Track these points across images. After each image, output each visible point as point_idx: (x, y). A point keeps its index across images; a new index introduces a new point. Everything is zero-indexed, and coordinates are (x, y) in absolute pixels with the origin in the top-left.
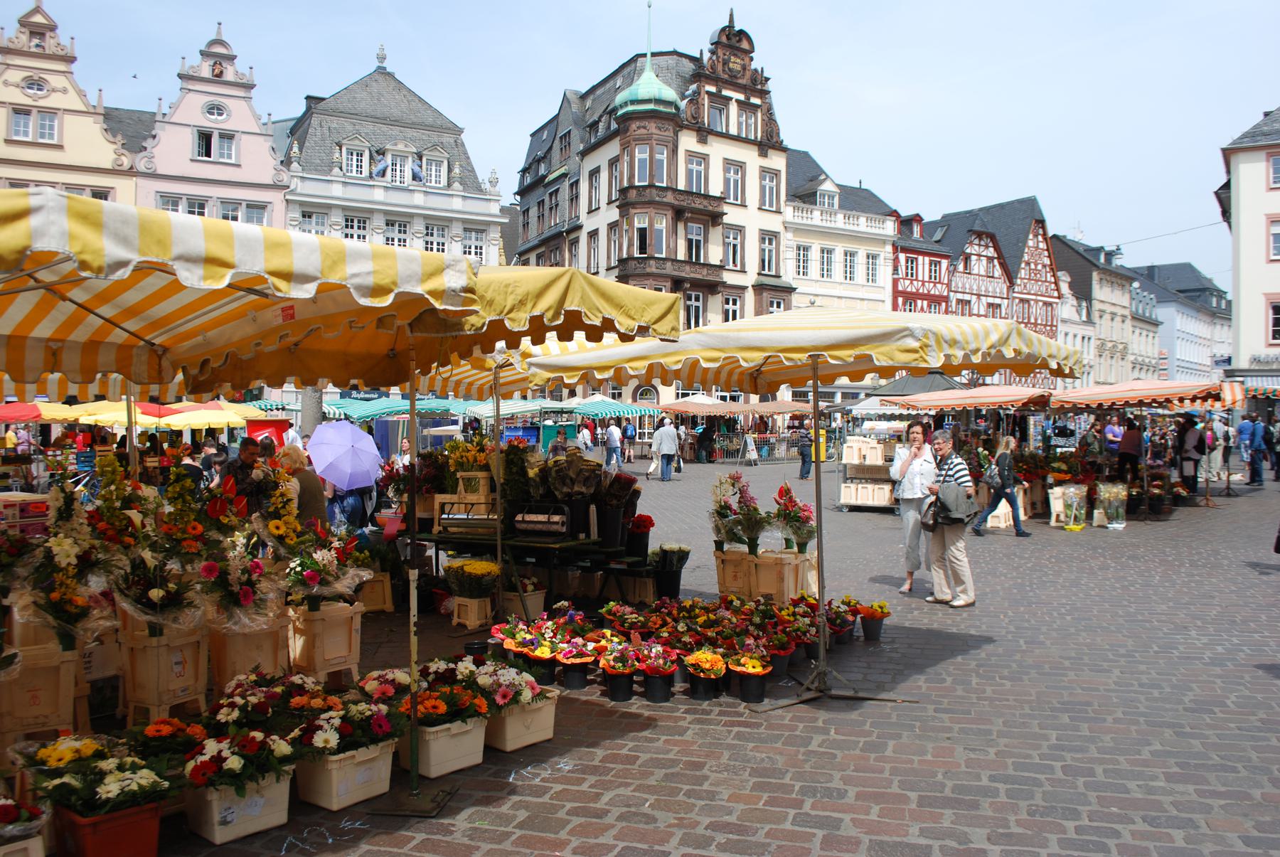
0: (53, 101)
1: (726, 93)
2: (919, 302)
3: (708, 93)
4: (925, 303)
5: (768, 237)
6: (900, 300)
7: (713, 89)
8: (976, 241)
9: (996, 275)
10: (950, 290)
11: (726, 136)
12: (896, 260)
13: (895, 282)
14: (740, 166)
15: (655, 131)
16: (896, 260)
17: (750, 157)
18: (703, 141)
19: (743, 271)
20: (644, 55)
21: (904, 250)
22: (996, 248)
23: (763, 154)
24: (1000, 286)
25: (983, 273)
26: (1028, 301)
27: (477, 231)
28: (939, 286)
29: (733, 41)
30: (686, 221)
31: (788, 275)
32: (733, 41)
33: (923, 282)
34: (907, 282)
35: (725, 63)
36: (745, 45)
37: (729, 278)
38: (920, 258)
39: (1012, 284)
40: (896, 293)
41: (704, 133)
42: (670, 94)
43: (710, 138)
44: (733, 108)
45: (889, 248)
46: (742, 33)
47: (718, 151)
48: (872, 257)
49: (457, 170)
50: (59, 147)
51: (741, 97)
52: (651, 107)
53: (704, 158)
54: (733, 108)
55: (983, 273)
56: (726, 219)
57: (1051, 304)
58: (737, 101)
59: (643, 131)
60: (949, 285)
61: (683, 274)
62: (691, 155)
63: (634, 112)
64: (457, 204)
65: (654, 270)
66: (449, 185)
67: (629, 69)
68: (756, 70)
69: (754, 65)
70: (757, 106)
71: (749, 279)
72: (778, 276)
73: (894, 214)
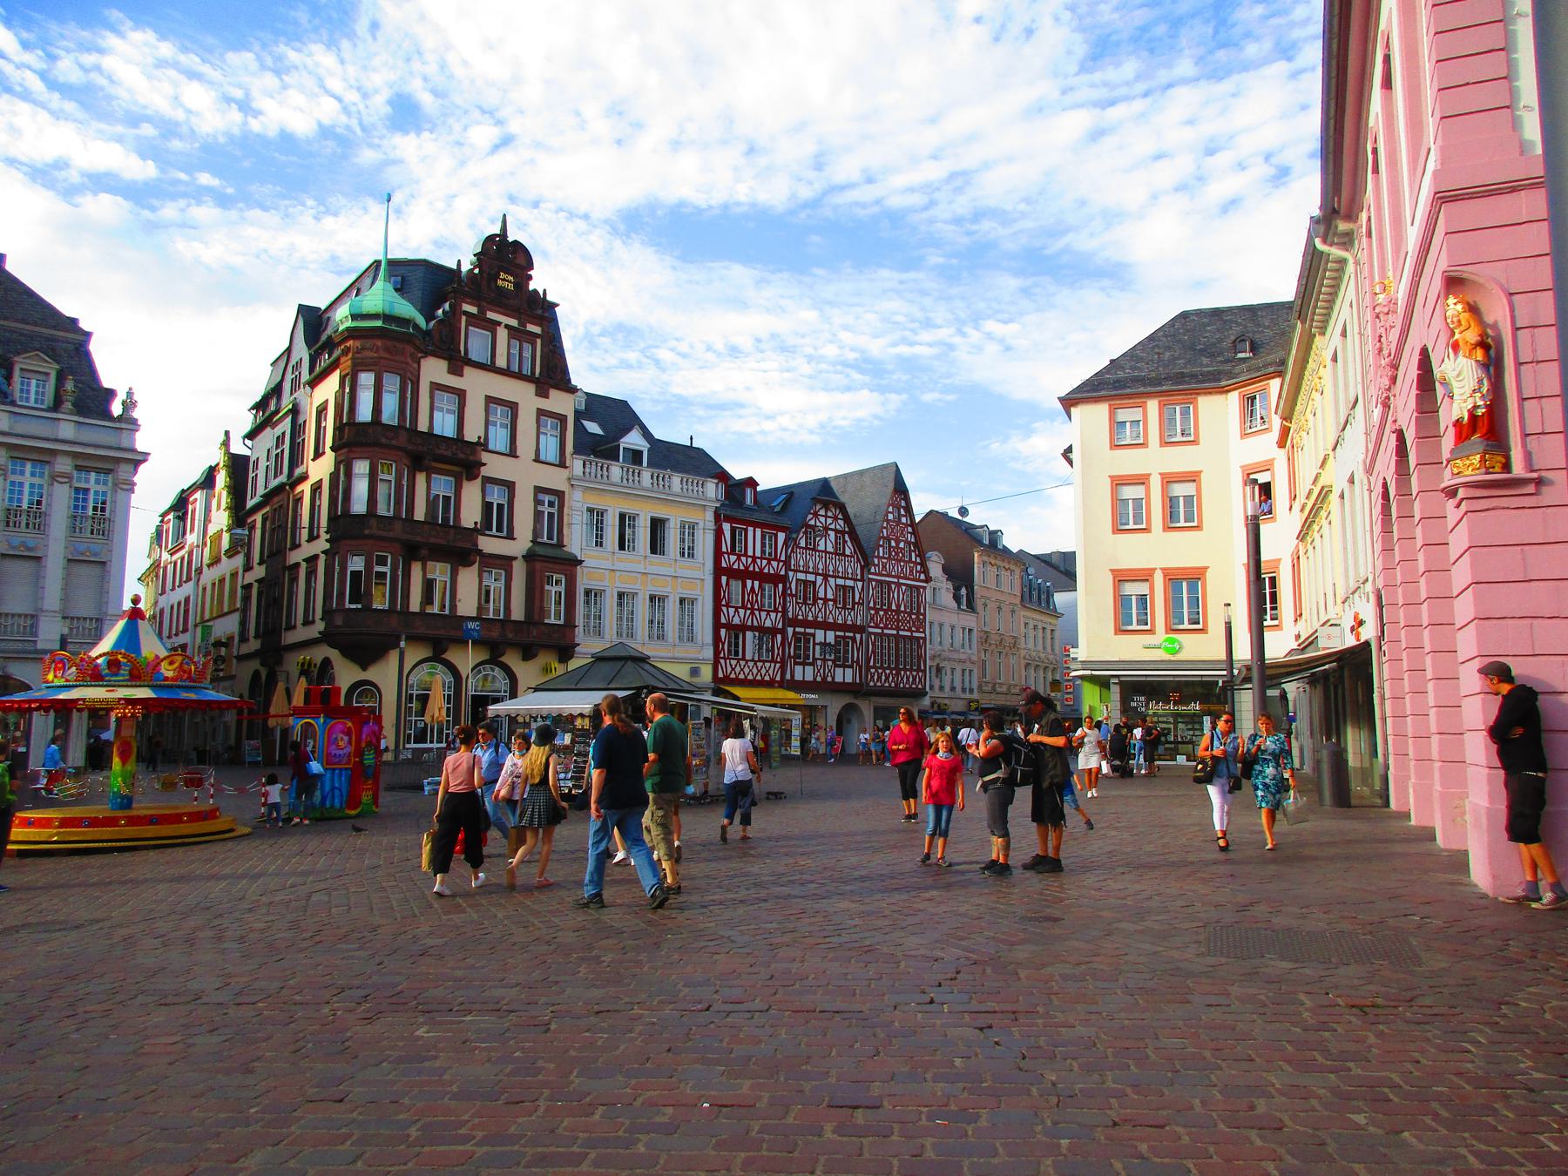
1: (491, 315)
2: (749, 583)
3: (466, 313)
4: (756, 583)
6: (724, 579)
7: (473, 310)
8: (822, 512)
9: (848, 552)
10: (788, 568)
11: (491, 368)
13: (718, 554)
14: (513, 407)
16: (719, 533)
17: (523, 394)
18: (456, 370)
19: (510, 536)
21: (728, 519)
22: (847, 519)
23: (542, 393)
24: (853, 567)
25: (830, 549)
26: (889, 583)
27: (98, 471)
28: (774, 564)
30: (430, 472)
33: (754, 558)
34: (733, 558)
37: (488, 545)
38: (751, 529)
39: (866, 566)
40: (718, 571)
41: (458, 363)
42: (405, 309)
43: (468, 370)
44: (502, 334)
45: (710, 516)
47: (477, 384)
49: (69, 386)
51: (514, 323)
52: (379, 323)
53: (461, 394)
54: (502, 334)
55: (830, 549)
56: (484, 471)
57: (918, 588)
58: (507, 326)
60: (787, 563)
61: (418, 539)
62: (436, 387)
64: (67, 430)
65: (374, 531)
66: (57, 406)
68: (535, 291)
69: (532, 286)
70: (536, 335)
72: (560, 545)
73: (723, 476)
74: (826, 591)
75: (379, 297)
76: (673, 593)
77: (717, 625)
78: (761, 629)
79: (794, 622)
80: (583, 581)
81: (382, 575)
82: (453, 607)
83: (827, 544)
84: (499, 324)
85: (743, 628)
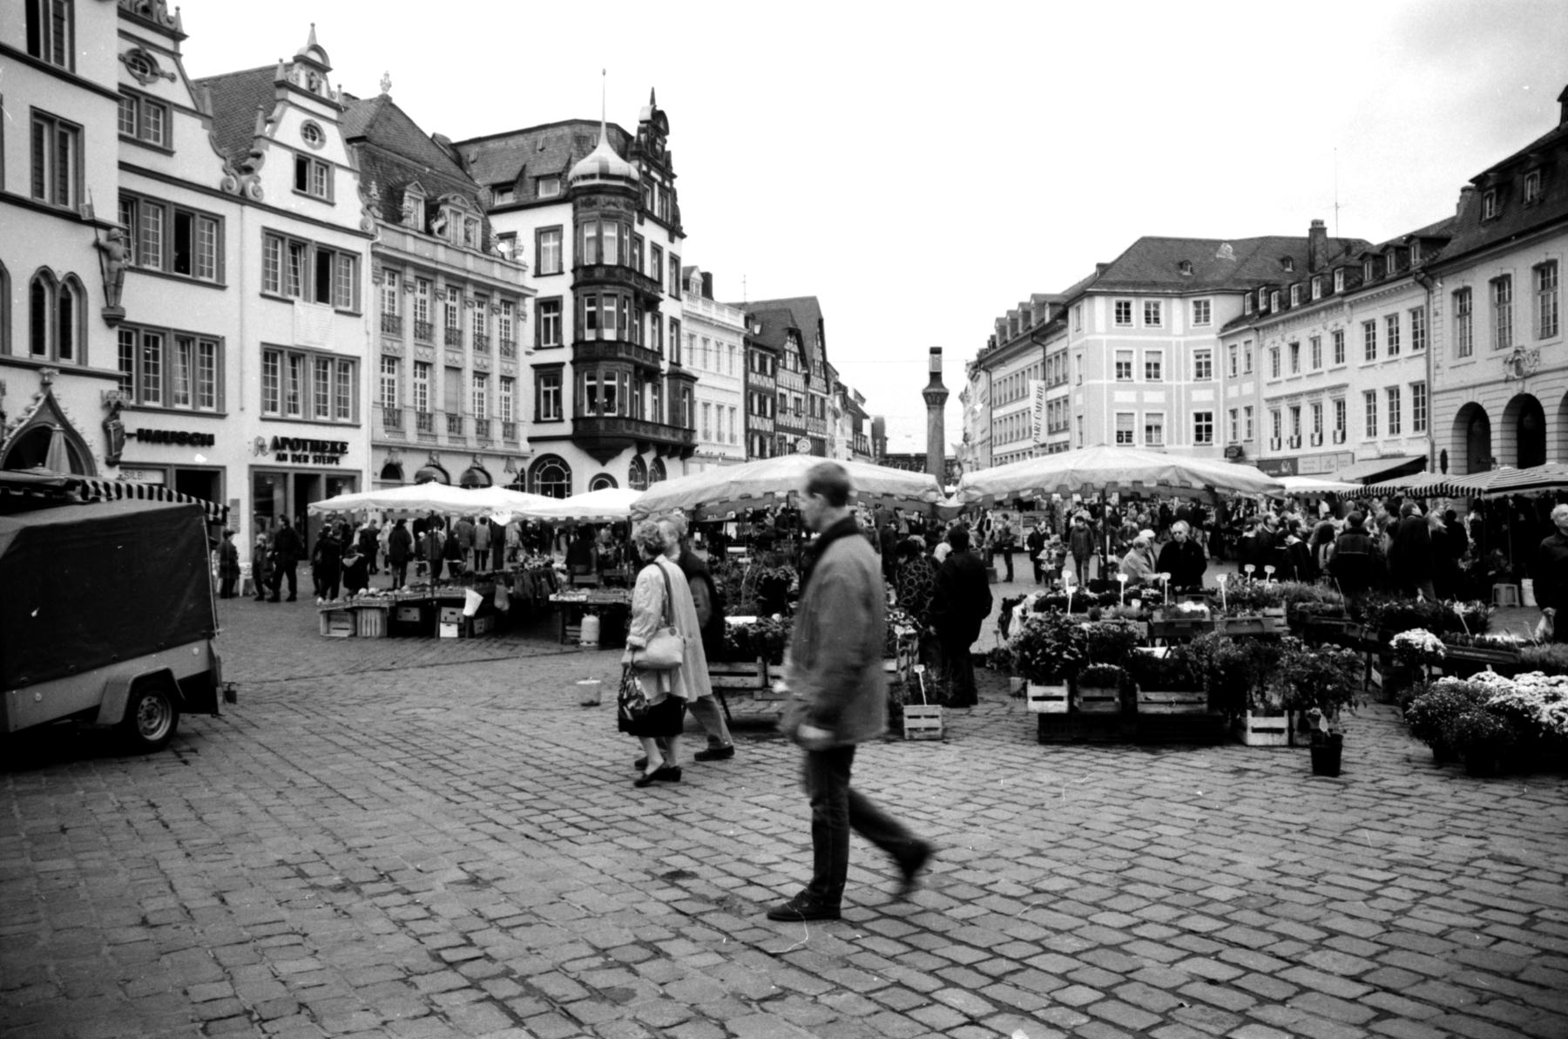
0: (161, 89)
5: (675, 323)
15: (622, 209)
20: (597, 124)
23: (671, 240)
24: (799, 382)
29: (657, 124)
31: (685, 367)
32: (657, 124)
35: (653, 142)
36: (662, 126)
43: (647, 222)
45: (741, 341)
48: (731, 348)
50: (168, 152)
52: (622, 184)
59: (612, 208)
63: (605, 186)
67: (581, 134)
71: (665, 366)
74: (790, 403)
75: (604, 155)
77: (747, 430)
79: (777, 427)
80: (699, 394)
84: (654, 180)
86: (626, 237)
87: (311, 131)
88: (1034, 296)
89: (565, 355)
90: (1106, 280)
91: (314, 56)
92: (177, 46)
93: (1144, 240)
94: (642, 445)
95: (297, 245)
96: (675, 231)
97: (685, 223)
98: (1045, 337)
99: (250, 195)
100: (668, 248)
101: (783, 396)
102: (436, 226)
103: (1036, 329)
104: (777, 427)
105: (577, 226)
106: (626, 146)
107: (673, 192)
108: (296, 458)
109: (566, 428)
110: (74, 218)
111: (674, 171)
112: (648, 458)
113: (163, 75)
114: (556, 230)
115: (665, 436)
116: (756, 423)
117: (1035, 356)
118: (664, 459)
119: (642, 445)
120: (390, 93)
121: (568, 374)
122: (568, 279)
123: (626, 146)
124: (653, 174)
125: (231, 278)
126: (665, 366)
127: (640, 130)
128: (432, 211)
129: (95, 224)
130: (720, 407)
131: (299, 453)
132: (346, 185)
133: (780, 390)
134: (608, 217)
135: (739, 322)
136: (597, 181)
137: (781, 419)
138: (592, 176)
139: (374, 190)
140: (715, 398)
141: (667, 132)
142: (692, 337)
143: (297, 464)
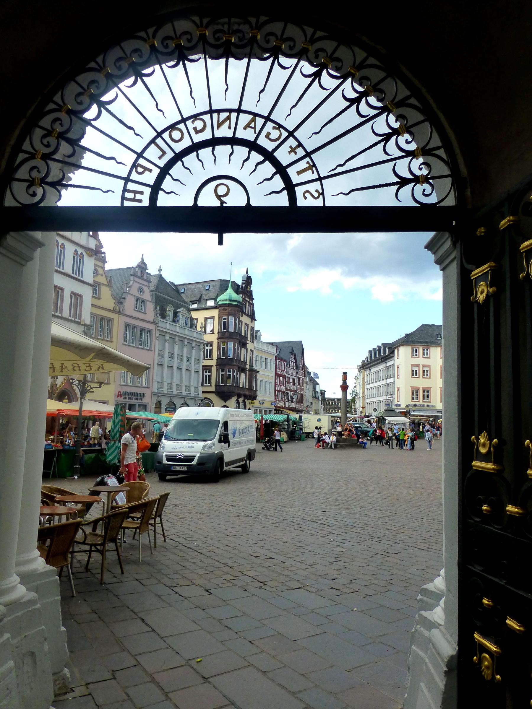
12: (276, 362)
16: (276, 362)
21: (279, 359)
23: (252, 322)
24: (294, 373)
29: (248, 280)
31: (254, 367)
35: (247, 287)
40: (276, 374)
46: (250, 277)
48: (271, 360)
52: (236, 303)
67: (224, 285)
74: (291, 381)
76: (268, 380)
77: (275, 390)
78: (281, 391)
79: (286, 389)
80: (259, 377)
81: (230, 375)
82: (239, 385)
83: (292, 365)
84: (247, 301)
85: (279, 391)
86: (237, 322)
87: (140, 290)
88: (383, 344)
89: (214, 362)
90: (408, 340)
91: (143, 266)
92: (104, 265)
93: (423, 325)
94: (239, 396)
95: (134, 327)
96: (253, 318)
97: (256, 315)
98: (386, 360)
99: (121, 311)
100: (250, 324)
101: (288, 378)
102: (176, 319)
103: (382, 355)
104: (286, 389)
105: (220, 317)
106: (237, 289)
107: (253, 305)
108: (129, 398)
109: (213, 389)
110: (79, 323)
111: (253, 297)
112: (241, 400)
113: (99, 274)
114: (213, 318)
115: (247, 393)
116: (278, 388)
117: (383, 366)
118: (246, 401)
119: (239, 396)
120: (161, 273)
121: (214, 369)
122: (216, 336)
123: (237, 289)
124: (246, 299)
125: (114, 339)
126: (248, 367)
127: (242, 284)
128: (175, 314)
129: (85, 325)
130: (266, 382)
131: (130, 396)
132: (150, 306)
133: (287, 376)
134: (230, 314)
135: (273, 350)
136: (228, 302)
137: (288, 386)
138: (226, 300)
139: (158, 309)
140: (264, 379)
141: (251, 283)
142: (257, 356)
143: (129, 401)
